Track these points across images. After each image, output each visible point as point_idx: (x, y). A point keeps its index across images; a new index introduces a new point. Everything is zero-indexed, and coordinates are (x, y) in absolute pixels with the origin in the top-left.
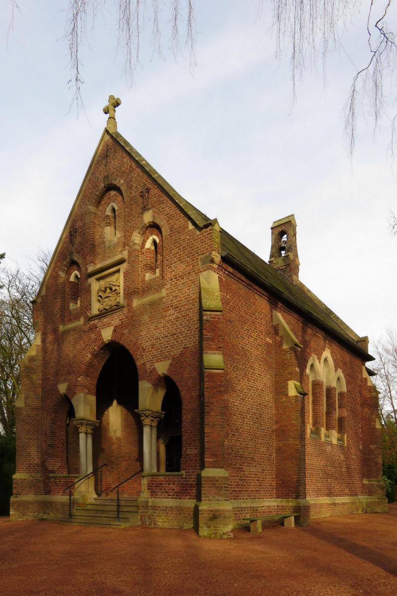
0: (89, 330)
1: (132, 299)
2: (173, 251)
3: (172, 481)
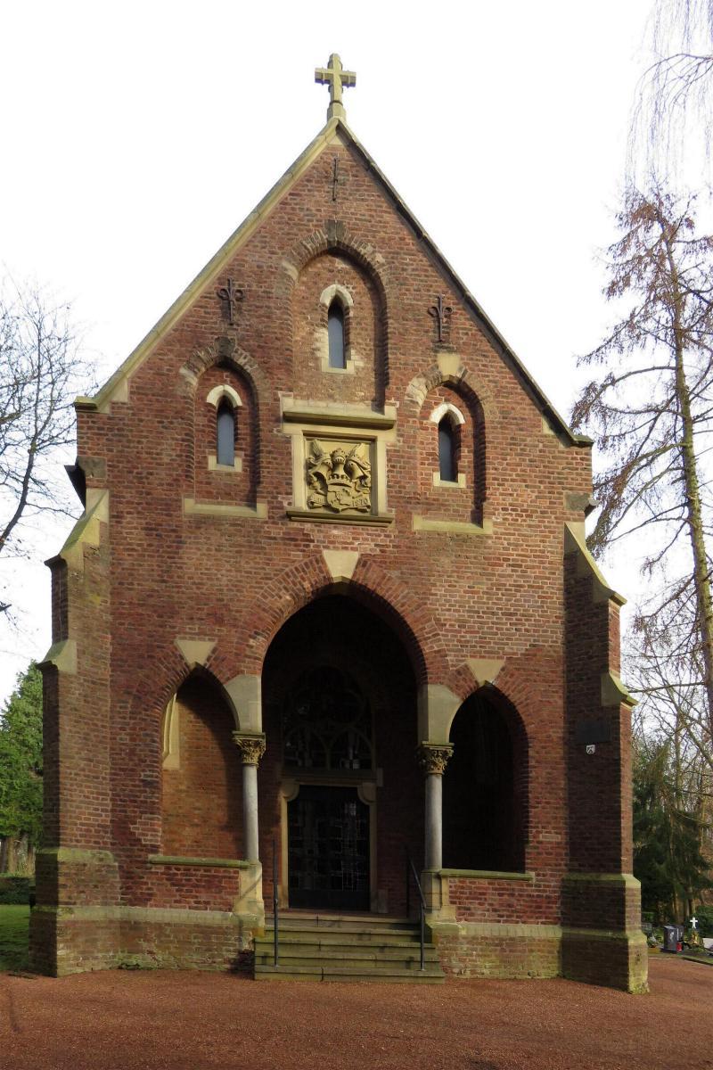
2: (509, 457)
3: (507, 890)
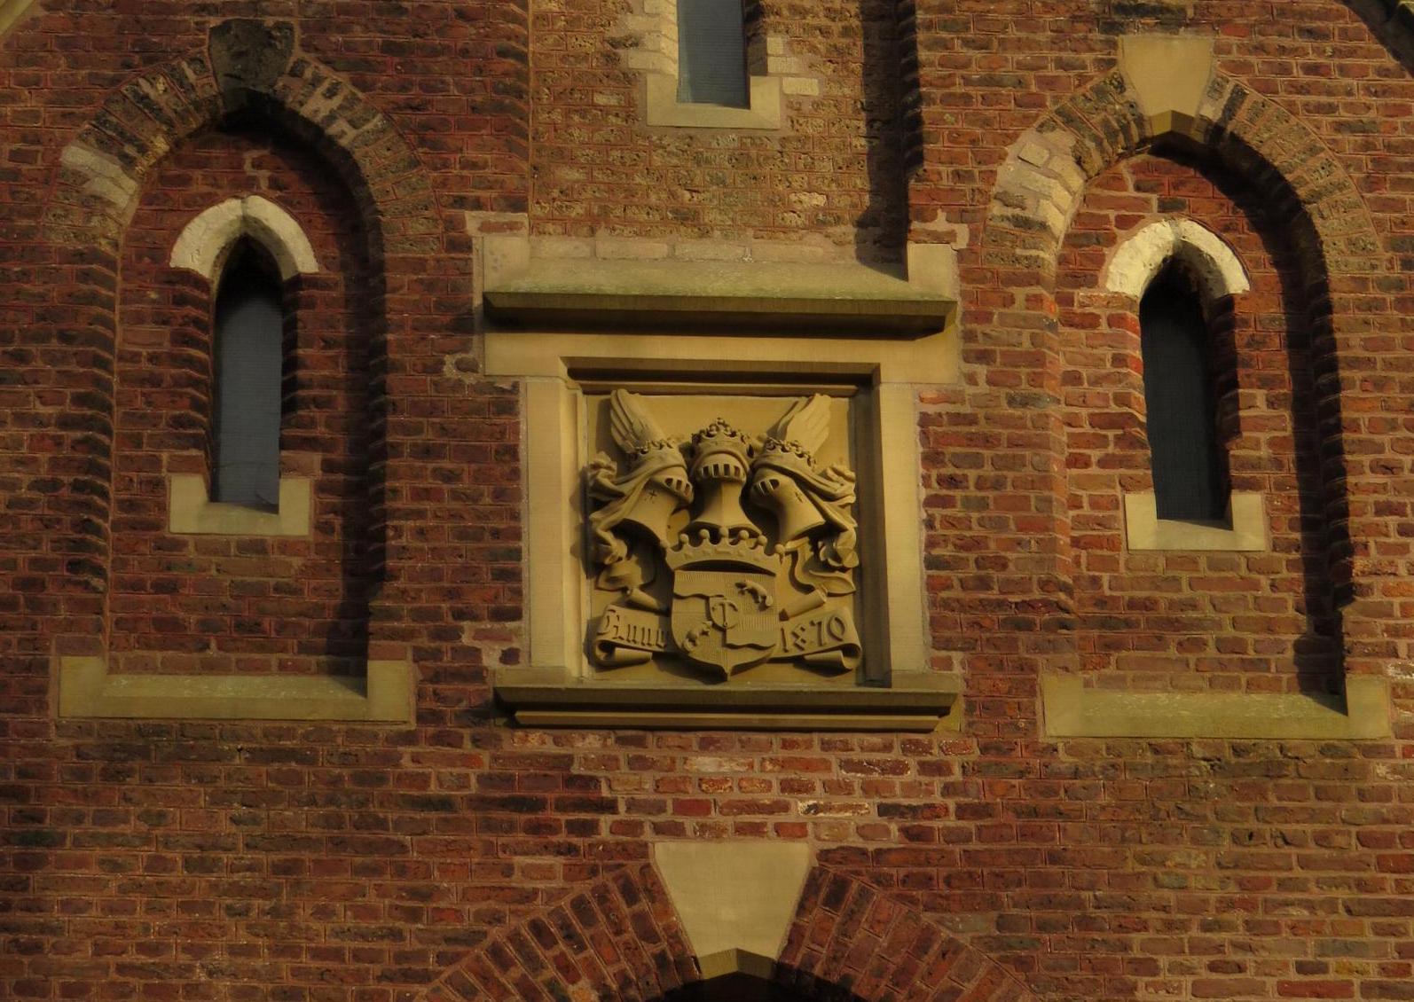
0: (480, 803)
1: (1028, 667)
